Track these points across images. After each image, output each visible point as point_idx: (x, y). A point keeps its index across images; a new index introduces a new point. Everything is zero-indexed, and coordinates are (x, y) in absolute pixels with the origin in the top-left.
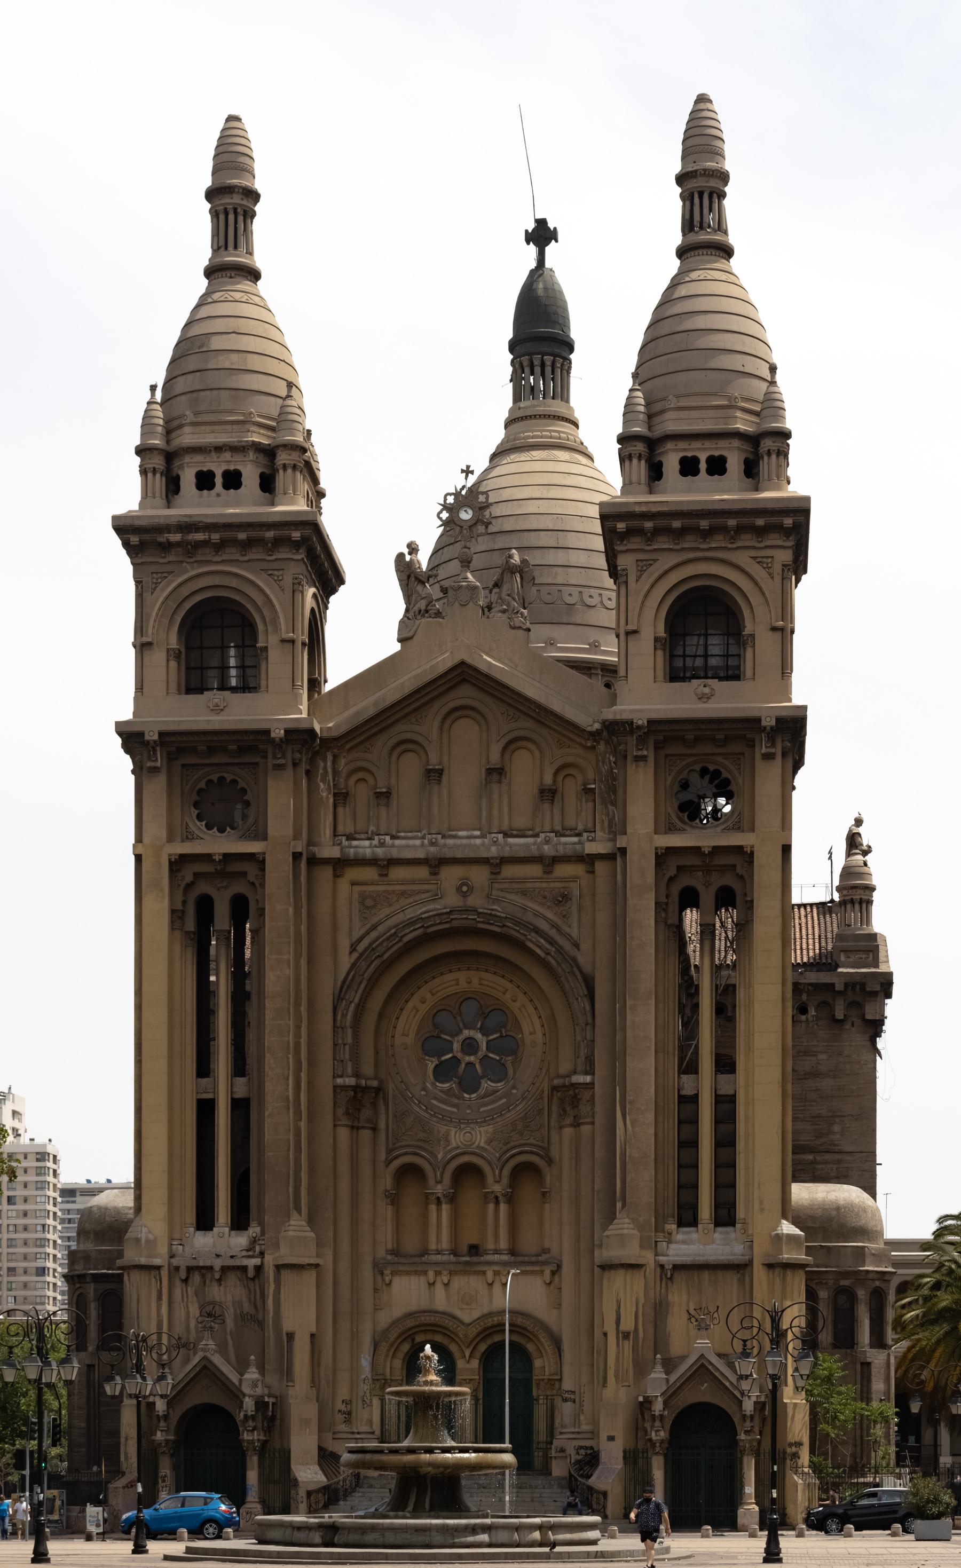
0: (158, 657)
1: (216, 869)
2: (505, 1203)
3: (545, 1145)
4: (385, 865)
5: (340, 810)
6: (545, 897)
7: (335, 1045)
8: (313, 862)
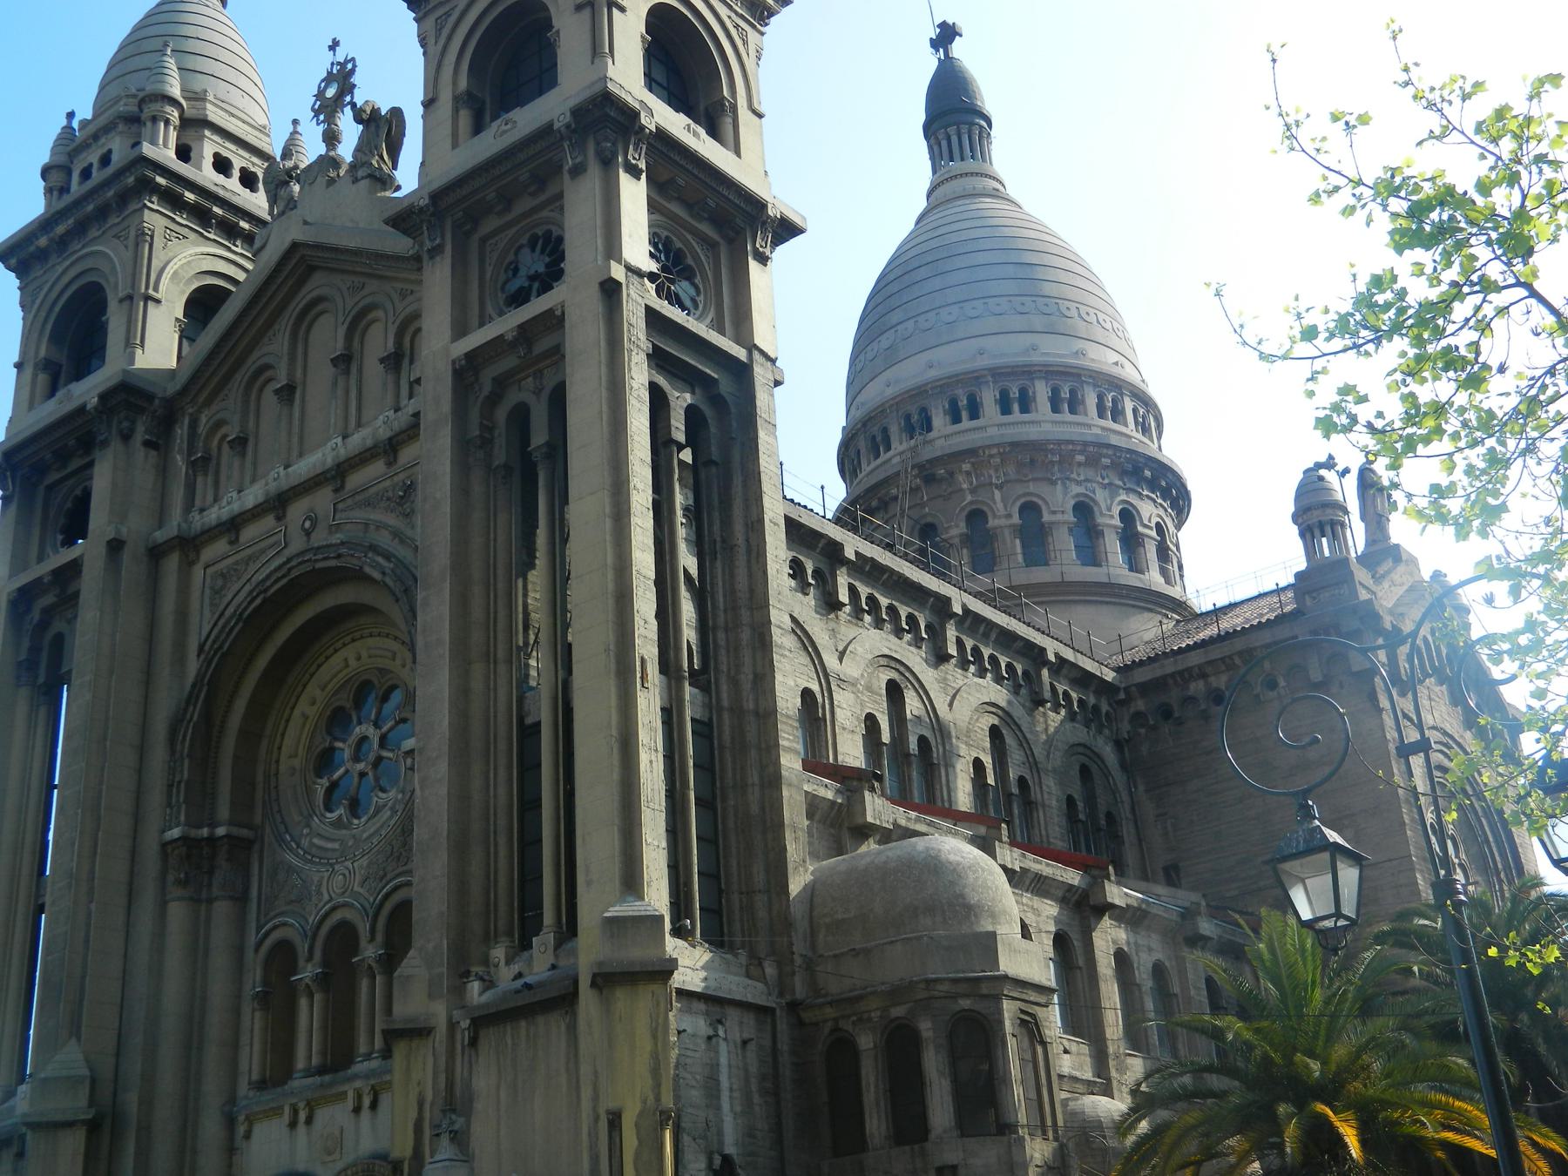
0: (29, 371)
1: (55, 596)
2: (379, 973)
4: (233, 526)
5: (200, 479)
6: (388, 499)
7: (170, 786)
8: (156, 554)
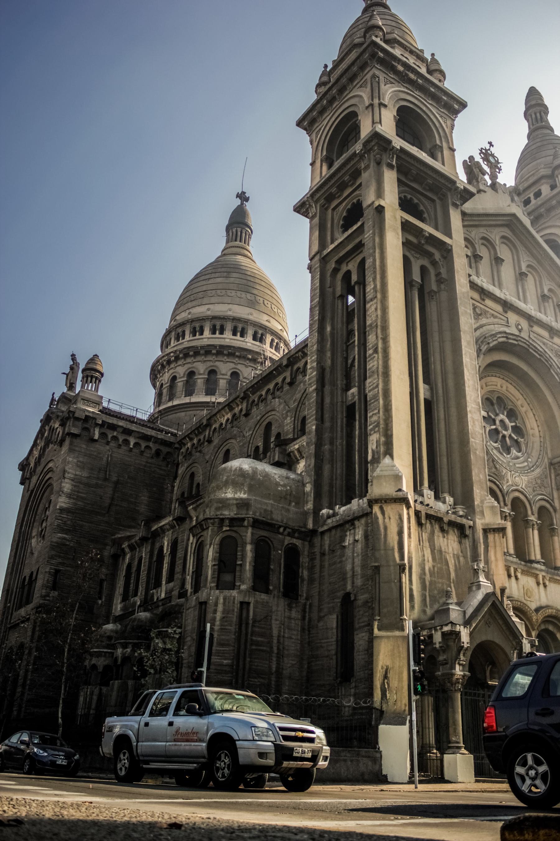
3: (551, 498)
